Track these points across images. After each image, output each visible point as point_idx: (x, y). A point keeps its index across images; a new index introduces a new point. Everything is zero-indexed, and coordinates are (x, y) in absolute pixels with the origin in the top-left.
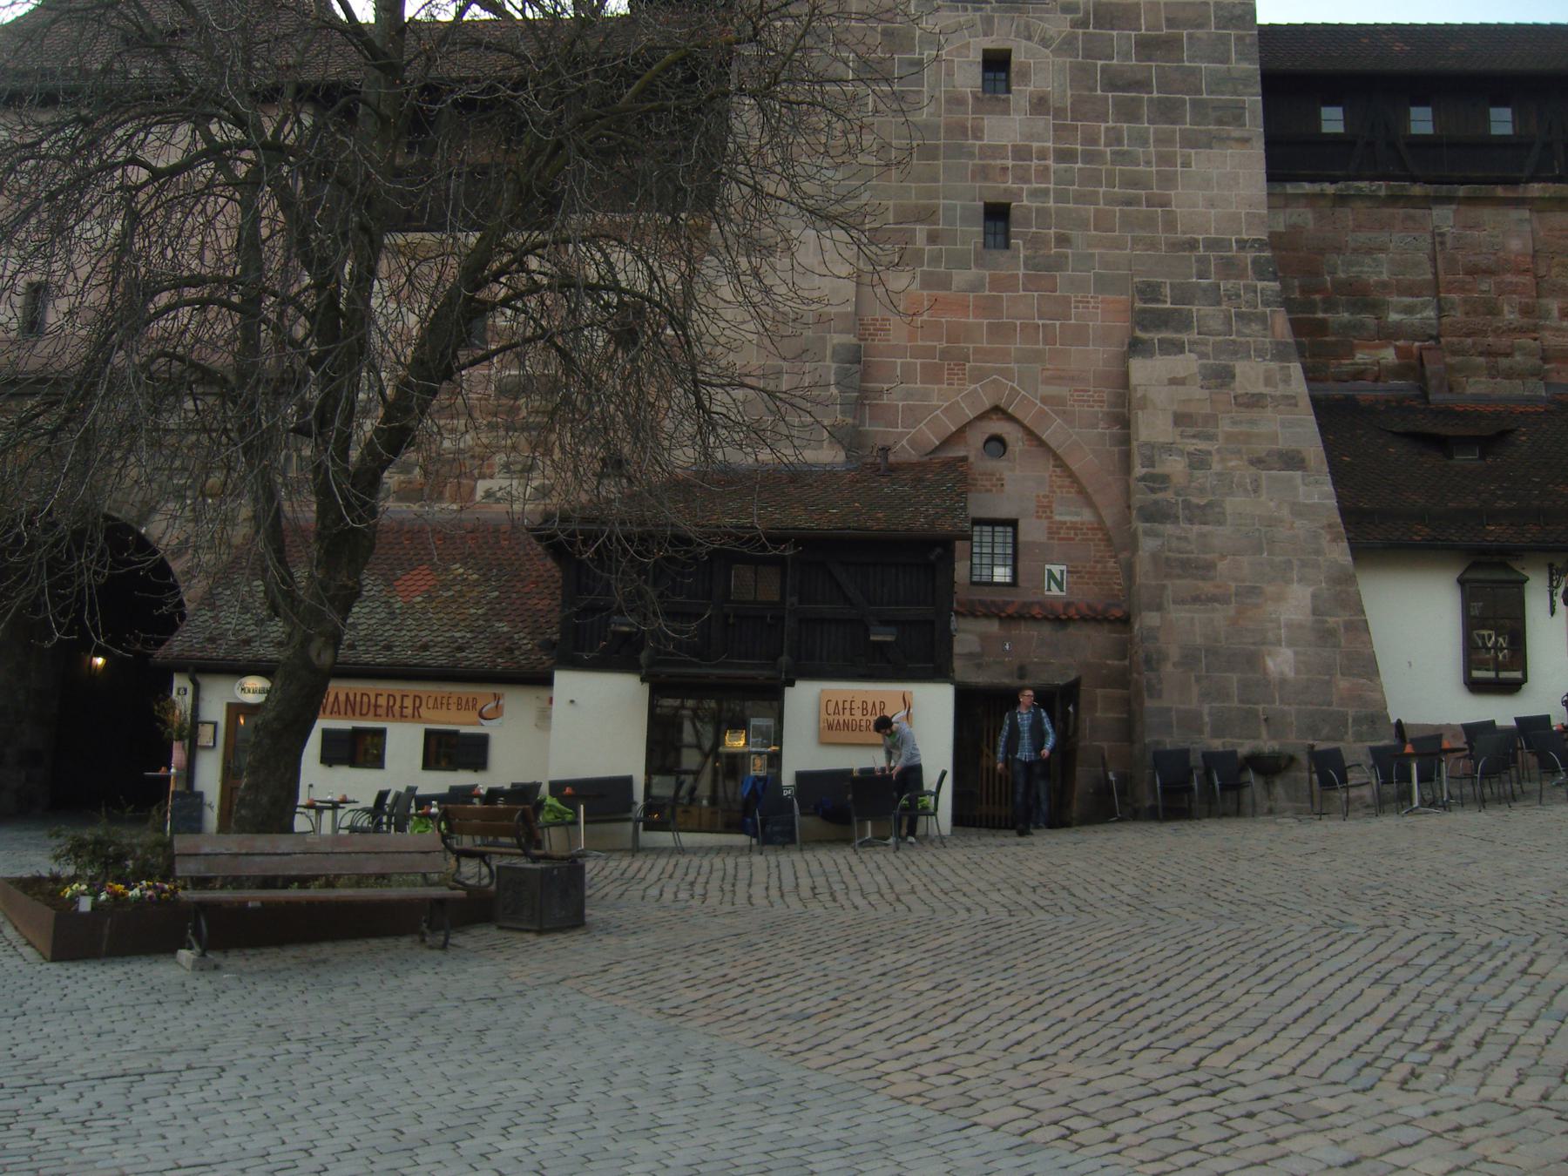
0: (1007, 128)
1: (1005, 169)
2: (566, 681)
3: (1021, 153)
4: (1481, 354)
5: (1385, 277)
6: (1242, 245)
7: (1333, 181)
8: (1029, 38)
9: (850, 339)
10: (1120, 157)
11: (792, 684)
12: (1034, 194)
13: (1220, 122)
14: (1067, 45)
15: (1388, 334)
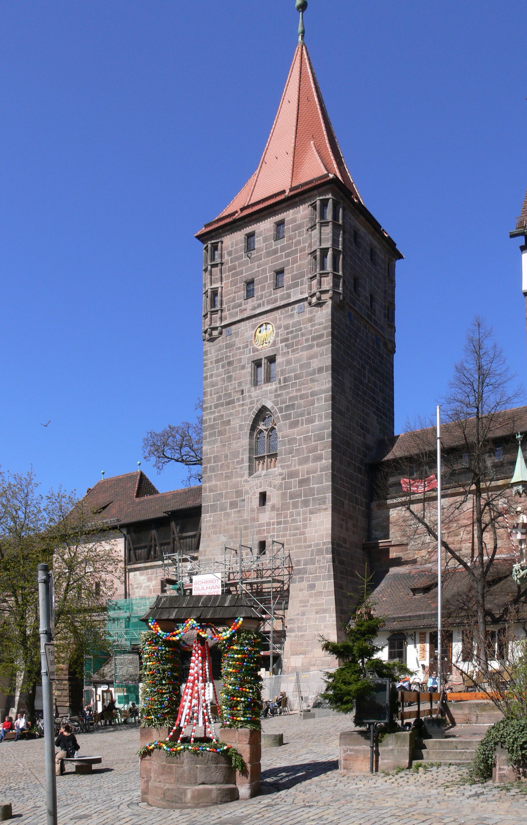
0: (266, 516)
1: (264, 530)
3: (268, 524)
8: (271, 487)
10: (294, 521)
13: (320, 504)
14: (280, 487)
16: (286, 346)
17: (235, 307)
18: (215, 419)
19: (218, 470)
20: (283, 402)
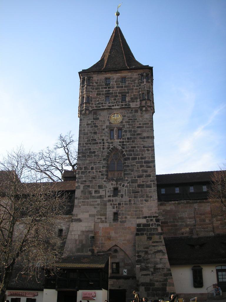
2: (45, 290)
4: (202, 228)
5: (187, 216)
6: (154, 217)
7: (177, 201)
9: (93, 235)
11: (78, 291)
12: (121, 211)
15: (187, 226)
16: (128, 124)
17: (99, 104)
18: (85, 150)
19: (87, 174)
20: (127, 148)
